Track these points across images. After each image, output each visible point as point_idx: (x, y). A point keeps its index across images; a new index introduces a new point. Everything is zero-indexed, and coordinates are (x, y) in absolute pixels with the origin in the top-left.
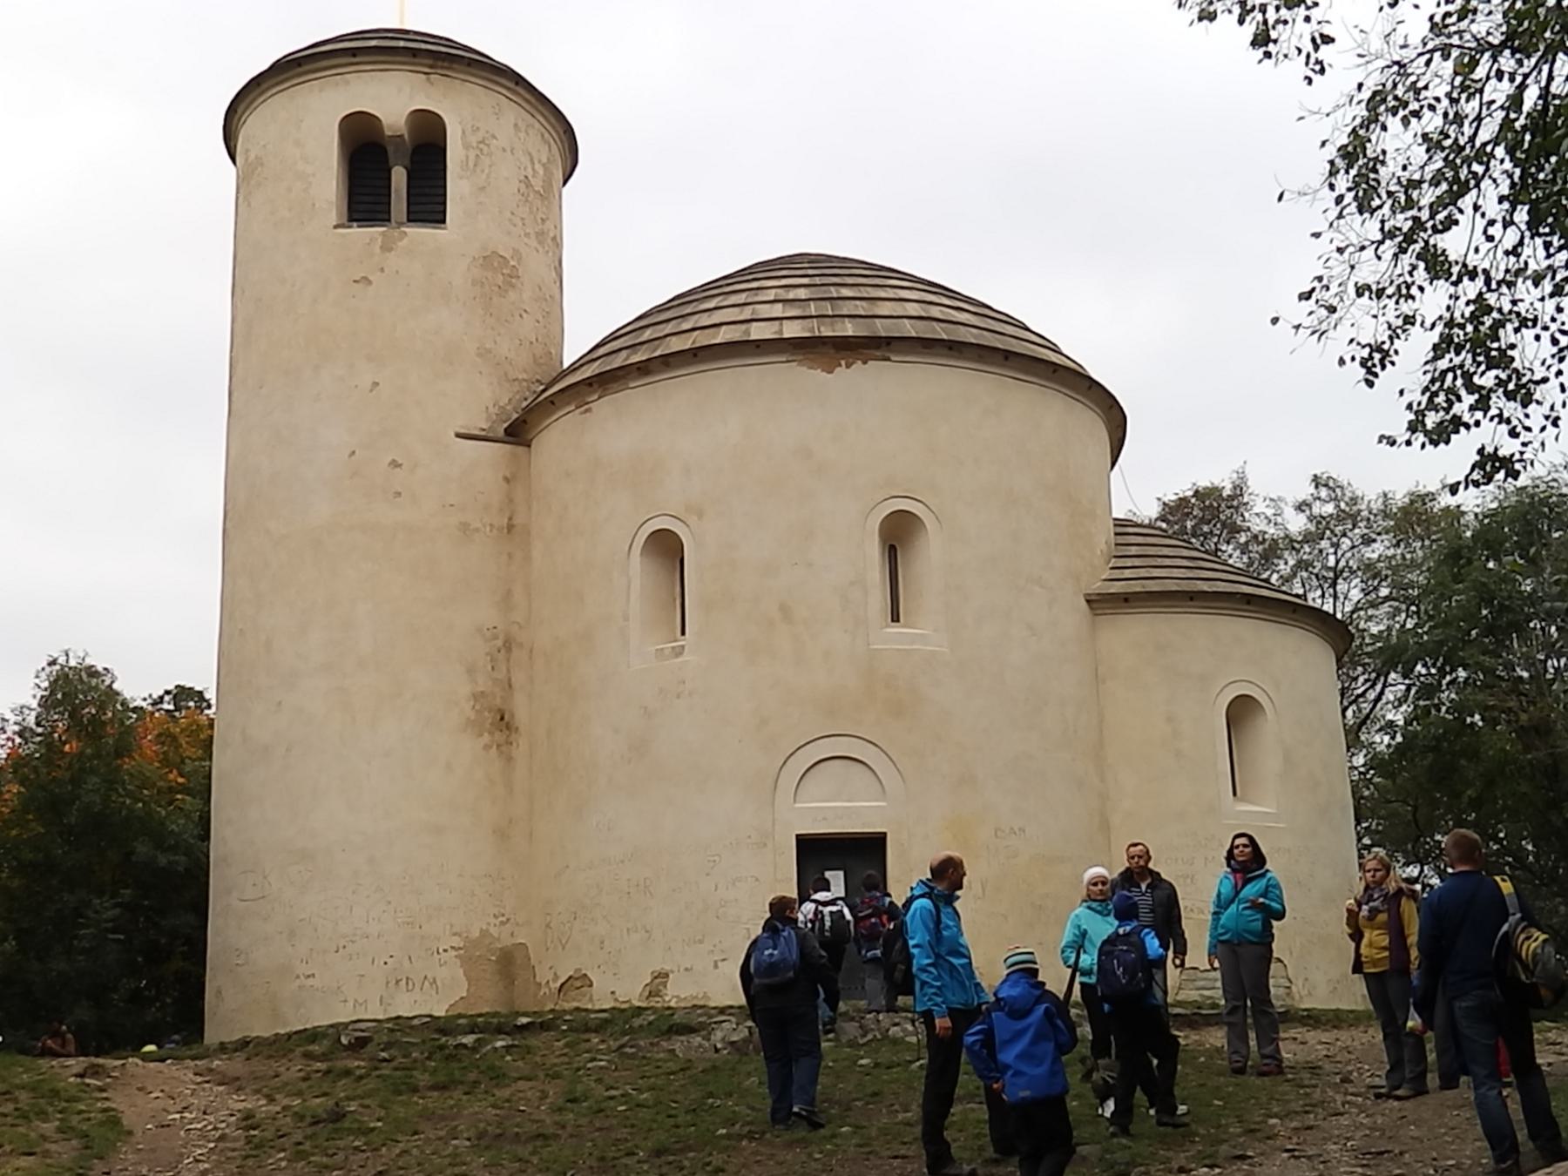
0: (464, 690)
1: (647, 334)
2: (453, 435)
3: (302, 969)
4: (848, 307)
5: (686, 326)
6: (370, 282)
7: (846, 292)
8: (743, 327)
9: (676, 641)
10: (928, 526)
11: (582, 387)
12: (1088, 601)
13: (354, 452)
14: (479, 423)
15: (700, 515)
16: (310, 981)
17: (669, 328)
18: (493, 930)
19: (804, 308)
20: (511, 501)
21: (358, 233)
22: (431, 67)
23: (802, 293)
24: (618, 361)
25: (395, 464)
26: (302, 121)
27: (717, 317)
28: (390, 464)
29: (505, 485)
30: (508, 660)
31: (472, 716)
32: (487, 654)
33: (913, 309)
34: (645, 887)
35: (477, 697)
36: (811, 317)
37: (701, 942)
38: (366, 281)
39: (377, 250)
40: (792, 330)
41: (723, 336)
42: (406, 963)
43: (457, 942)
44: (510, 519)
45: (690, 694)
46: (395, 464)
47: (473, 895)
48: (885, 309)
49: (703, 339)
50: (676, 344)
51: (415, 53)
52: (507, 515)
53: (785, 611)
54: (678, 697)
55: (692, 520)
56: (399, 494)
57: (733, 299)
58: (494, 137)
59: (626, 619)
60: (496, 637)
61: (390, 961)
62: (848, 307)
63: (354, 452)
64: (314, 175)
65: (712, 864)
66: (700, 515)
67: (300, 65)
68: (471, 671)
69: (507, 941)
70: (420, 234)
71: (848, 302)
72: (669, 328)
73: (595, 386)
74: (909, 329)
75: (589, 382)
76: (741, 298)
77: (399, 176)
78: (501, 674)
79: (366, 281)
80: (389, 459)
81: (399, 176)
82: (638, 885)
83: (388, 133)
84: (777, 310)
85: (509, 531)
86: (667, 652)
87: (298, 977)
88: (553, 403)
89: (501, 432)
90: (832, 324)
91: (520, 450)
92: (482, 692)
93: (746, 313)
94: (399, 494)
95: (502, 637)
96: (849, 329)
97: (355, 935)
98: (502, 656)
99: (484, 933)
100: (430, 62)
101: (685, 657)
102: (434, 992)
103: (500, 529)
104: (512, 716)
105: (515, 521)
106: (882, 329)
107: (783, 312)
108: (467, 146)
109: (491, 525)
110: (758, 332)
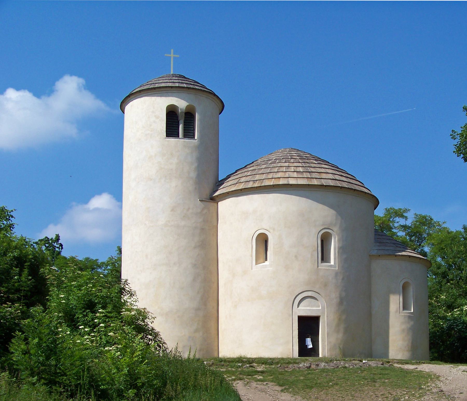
1: (257, 177)
4: (314, 175)
7: (313, 170)
11: (240, 191)
17: (264, 176)
21: (172, 140)
23: (301, 169)
24: (250, 185)
27: (279, 175)
33: (331, 176)
36: (305, 178)
41: (282, 182)
48: (324, 176)
57: (282, 169)
62: (314, 175)
71: (314, 173)
72: (264, 176)
74: (331, 183)
84: (295, 175)
90: (311, 181)
93: (287, 175)
96: (315, 182)
106: (324, 182)
107: (297, 176)
110: (292, 182)
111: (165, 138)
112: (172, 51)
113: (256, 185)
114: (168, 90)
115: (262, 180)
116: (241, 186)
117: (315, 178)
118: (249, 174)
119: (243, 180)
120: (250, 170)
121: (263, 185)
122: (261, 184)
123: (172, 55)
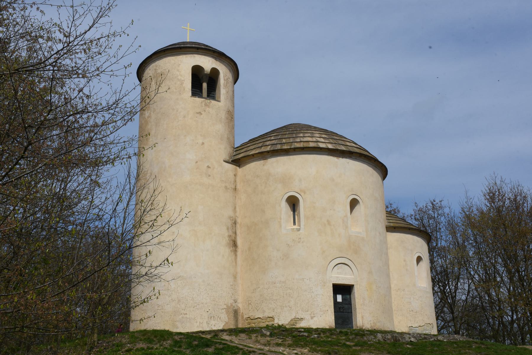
0: (227, 234)
2: (222, 160)
3: (183, 312)
5: (298, 140)
6: (201, 114)
8: (316, 143)
9: (292, 227)
10: (361, 203)
11: (265, 153)
12: (386, 227)
13: (197, 162)
14: (227, 158)
15: (305, 193)
16: (186, 316)
17: (291, 140)
18: (234, 305)
19: (329, 140)
20: (236, 181)
21: (197, 100)
22: (217, 56)
24: (279, 147)
25: (208, 167)
26: (180, 65)
28: (207, 167)
29: (234, 176)
30: (235, 227)
31: (228, 241)
32: (231, 224)
34: (289, 295)
35: (230, 236)
37: (308, 311)
38: (200, 113)
39: (203, 105)
40: (330, 146)
41: (312, 145)
42: (213, 312)
43: (225, 307)
44: (235, 186)
45: (303, 242)
46: (208, 167)
47: (229, 293)
49: (306, 145)
50: (298, 145)
51: (198, 48)
52: (235, 185)
53: (329, 222)
54: (299, 242)
55: (302, 194)
56: (209, 176)
58: (229, 78)
59: (281, 219)
60: (233, 220)
61: (209, 311)
63: (197, 162)
64: (184, 81)
65: (310, 290)
66: (305, 193)
67: (181, 49)
68: (228, 229)
69: (236, 308)
70: (213, 102)
72: (291, 140)
73: (270, 153)
75: (268, 152)
76: (309, 135)
77: (205, 85)
78: (234, 231)
79: (200, 113)
80: (207, 165)
81: (205, 85)
82: (287, 294)
83: (206, 73)
84: (322, 140)
85: (235, 190)
86: (295, 230)
87: (182, 314)
88: (253, 156)
89: (230, 161)
90: (339, 146)
91: (238, 168)
92: (231, 235)
94: (209, 176)
95: (234, 220)
97: (199, 303)
98: (234, 225)
99: (232, 305)
100: (217, 55)
101: (301, 231)
102: (220, 321)
103: (233, 189)
104: (236, 243)
105: (237, 188)
108: (224, 80)
109: (232, 188)
110: (322, 145)
111: (191, 97)
112: (188, 24)
113: (285, 147)
114: (193, 51)
115: (290, 144)
116: (268, 149)
117: (342, 145)
118: (273, 138)
119: (268, 143)
120: (273, 136)
121: (293, 147)
122: (291, 145)
123: (188, 28)
